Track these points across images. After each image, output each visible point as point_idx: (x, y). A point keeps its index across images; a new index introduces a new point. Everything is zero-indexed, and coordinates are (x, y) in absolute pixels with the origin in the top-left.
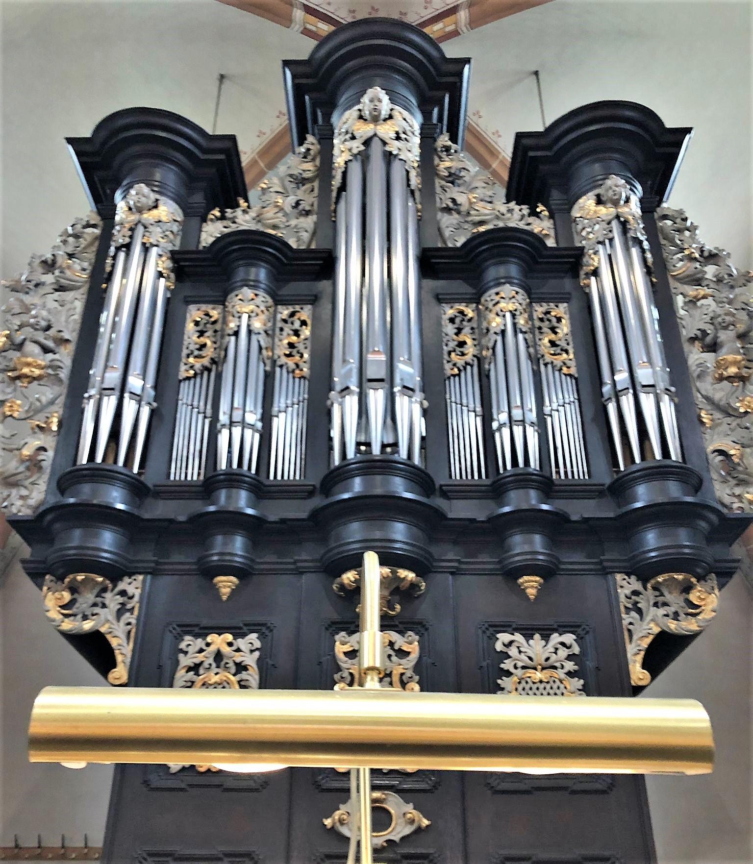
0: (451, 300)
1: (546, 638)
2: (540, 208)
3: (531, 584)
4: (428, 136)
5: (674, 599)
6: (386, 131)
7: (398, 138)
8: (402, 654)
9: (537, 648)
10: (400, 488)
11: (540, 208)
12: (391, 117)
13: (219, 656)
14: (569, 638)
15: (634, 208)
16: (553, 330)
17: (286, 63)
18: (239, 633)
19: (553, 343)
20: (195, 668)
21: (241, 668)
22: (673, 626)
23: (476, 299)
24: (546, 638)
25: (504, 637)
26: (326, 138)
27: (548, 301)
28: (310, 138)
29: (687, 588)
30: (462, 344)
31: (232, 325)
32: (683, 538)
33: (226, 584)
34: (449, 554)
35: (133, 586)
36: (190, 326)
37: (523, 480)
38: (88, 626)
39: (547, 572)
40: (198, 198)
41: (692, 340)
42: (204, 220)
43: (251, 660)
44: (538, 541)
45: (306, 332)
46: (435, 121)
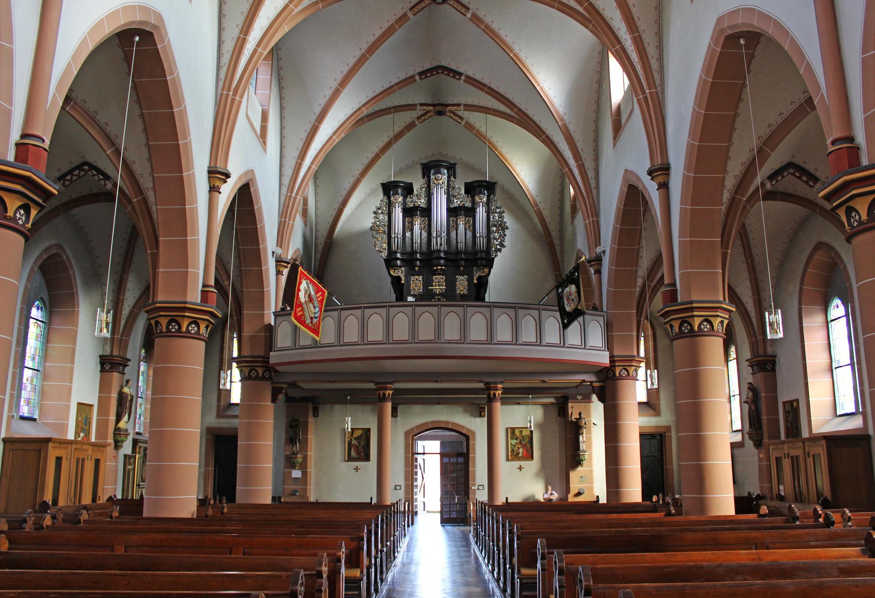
0: (452, 217)
1: (463, 276)
2: (469, 196)
3: (462, 268)
4: (449, 177)
5: (482, 271)
6: (441, 182)
7: (443, 183)
8: (443, 279)
9: (462, 278)
10: (442, 255)
11: (469, 196)
12: (441, 178)
13: (417, 279)
14: (466, 276)
15: (485, 199)
16: (469, 223)
17: (421, 164)
18: (419, 276)
19: (469, 226)
20: (413, 281)
21: (420, 281)
22: (481, 274)
23: (456, 217)
24: (463, 276)
25: (457, 276)
26: (429, 178)
27: (469, 217)
28: (426, 177)
29: (484, 269)
30: (453, 226)
31: (414, 223)
32: (484, 262)
33: (417, 268)
34: (450, 264)
35: (403, 269)
36: (406, 222)
37: (461, 252)
38: (397, 275)
39: (464, 267)
40: (405, 193)
41: (492, 226)
42: (407, 198)
43: (421, 280)
44: (463, 262)
45: (426, 223)
46: (450, 174)
